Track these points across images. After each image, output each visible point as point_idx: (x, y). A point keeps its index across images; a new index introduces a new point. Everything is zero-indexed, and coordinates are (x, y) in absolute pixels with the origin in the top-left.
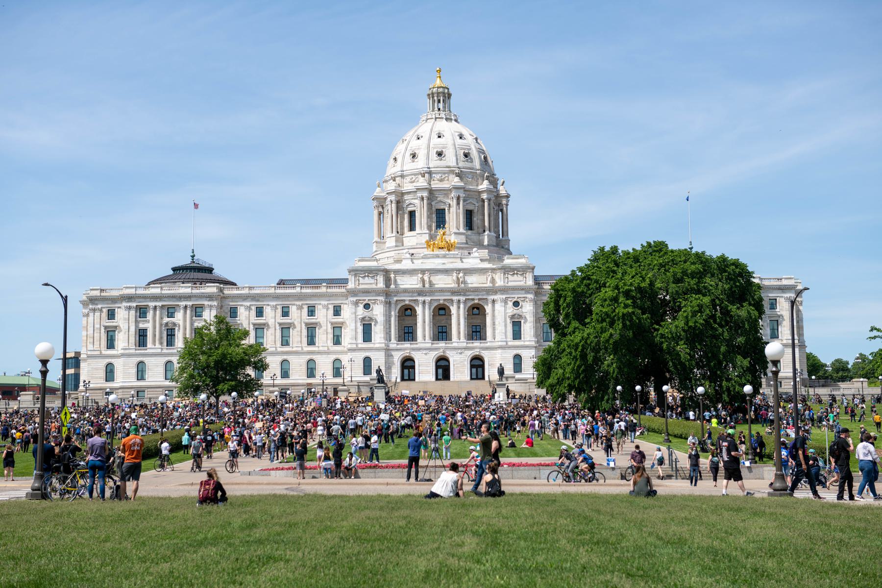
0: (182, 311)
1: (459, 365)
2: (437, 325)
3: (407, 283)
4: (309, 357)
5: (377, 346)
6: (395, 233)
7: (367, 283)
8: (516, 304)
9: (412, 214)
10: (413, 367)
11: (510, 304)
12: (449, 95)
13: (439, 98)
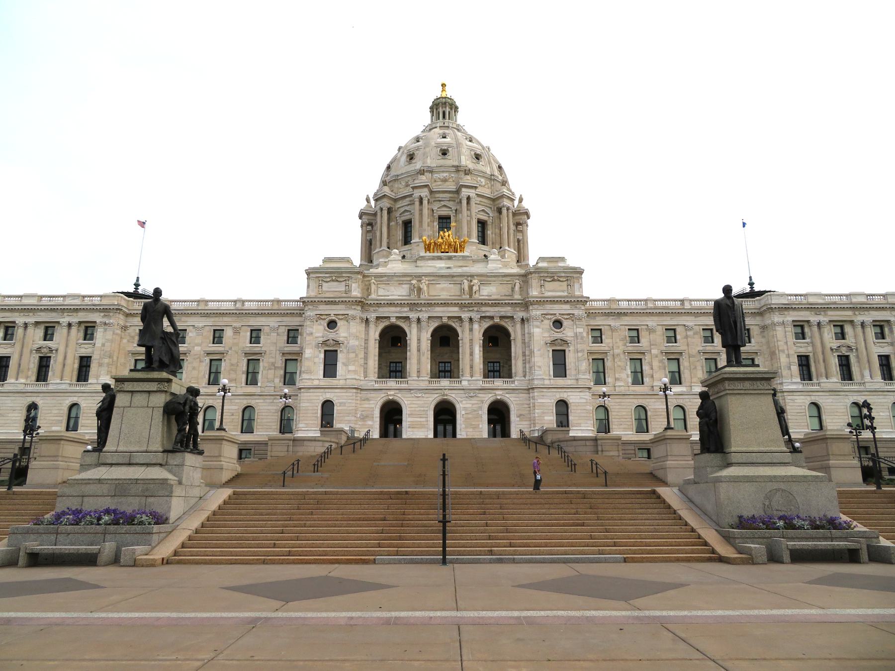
0: (65, 330)
1: (470, 416)
2: (438, 361)
3: (395, 293)
4: (245, 402)
5: (342, 383)
6: (384, 247)
7: (333, 289)
8: (558, 324)
9: (407, 225)
10: (400, 422)
11: (548, 323)
12: (457, 108)
13: (444, 109)
